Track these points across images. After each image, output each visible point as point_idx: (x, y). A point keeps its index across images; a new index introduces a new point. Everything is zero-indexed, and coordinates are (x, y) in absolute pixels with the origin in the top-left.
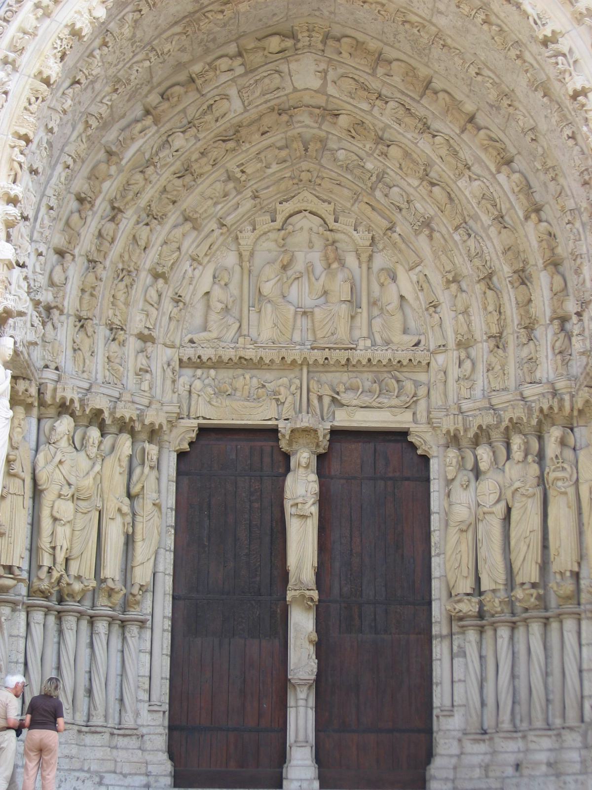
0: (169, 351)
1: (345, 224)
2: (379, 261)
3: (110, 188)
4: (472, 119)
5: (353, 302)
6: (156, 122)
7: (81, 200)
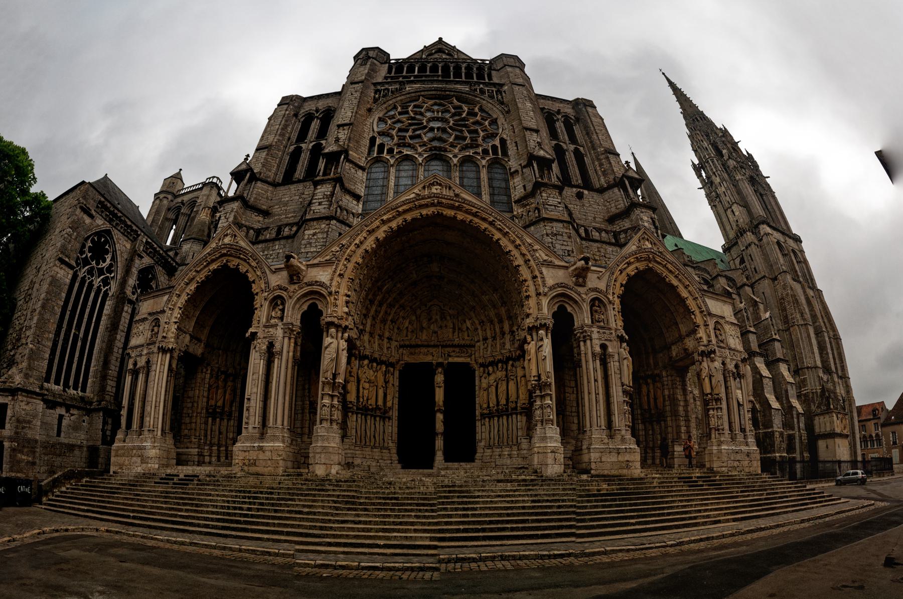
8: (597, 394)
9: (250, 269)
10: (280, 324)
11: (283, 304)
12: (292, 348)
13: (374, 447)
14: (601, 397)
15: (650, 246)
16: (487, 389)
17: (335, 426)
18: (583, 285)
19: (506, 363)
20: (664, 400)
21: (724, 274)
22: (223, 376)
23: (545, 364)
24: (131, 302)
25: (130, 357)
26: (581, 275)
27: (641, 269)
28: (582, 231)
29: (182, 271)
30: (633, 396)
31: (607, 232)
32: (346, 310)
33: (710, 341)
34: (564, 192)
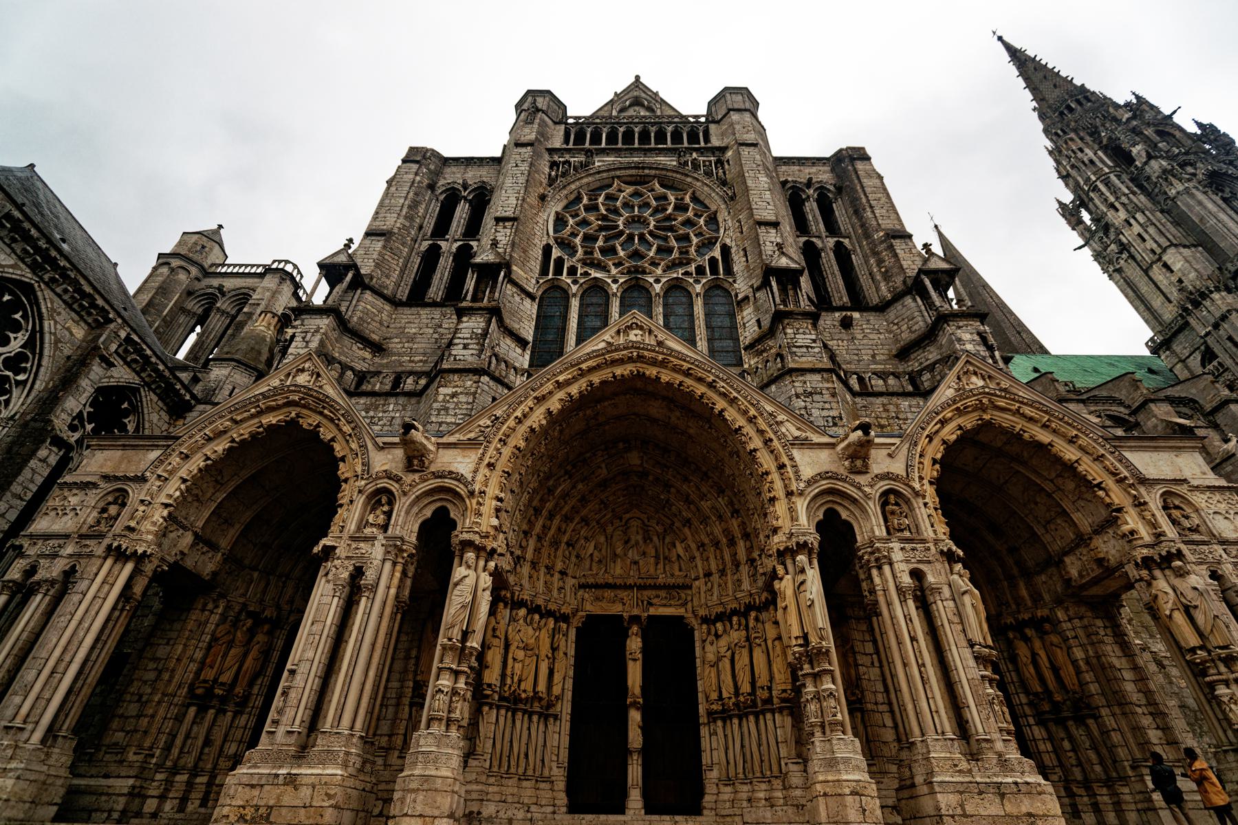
0: (574, 581)
1: (653, 523)
2: (668, 540)
3: (549, 505)
4: (706, 474)
5: (657, 557)
6: (570, 478)
7: (535, 509)
8: (921, 666)
9: (339, 437)
10: (381, 537)
11: (391, 503)
12: (396, 581)
13: (524, 777)
14: (931, 672)
15: (981, 383)
16: (715, 665)
17: (454, 733)
18: (864, 471)
19: (745, 615)
20: (1078, 672)
21: (1162, 395)
22: (249, 622)
23: (814, 615)
24: (58, 442)
25: (19, 552)
26: (858, 456)
27: (969, 426)
28: (853, 381)
29: (202, 412)
30: (1002, 666)
31: (897, 376)
32: (495, 522)
33: (1159, 536)
34: (821, 322)
